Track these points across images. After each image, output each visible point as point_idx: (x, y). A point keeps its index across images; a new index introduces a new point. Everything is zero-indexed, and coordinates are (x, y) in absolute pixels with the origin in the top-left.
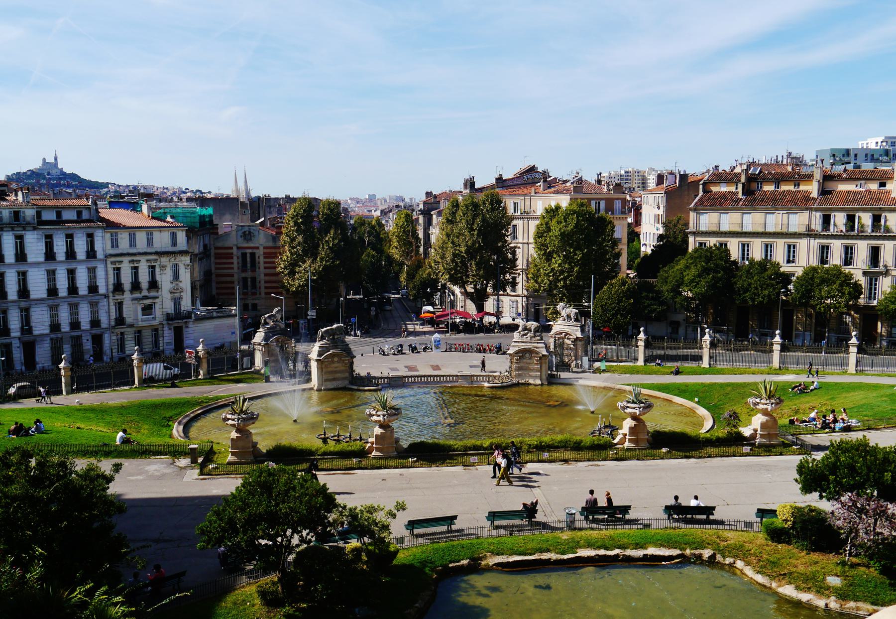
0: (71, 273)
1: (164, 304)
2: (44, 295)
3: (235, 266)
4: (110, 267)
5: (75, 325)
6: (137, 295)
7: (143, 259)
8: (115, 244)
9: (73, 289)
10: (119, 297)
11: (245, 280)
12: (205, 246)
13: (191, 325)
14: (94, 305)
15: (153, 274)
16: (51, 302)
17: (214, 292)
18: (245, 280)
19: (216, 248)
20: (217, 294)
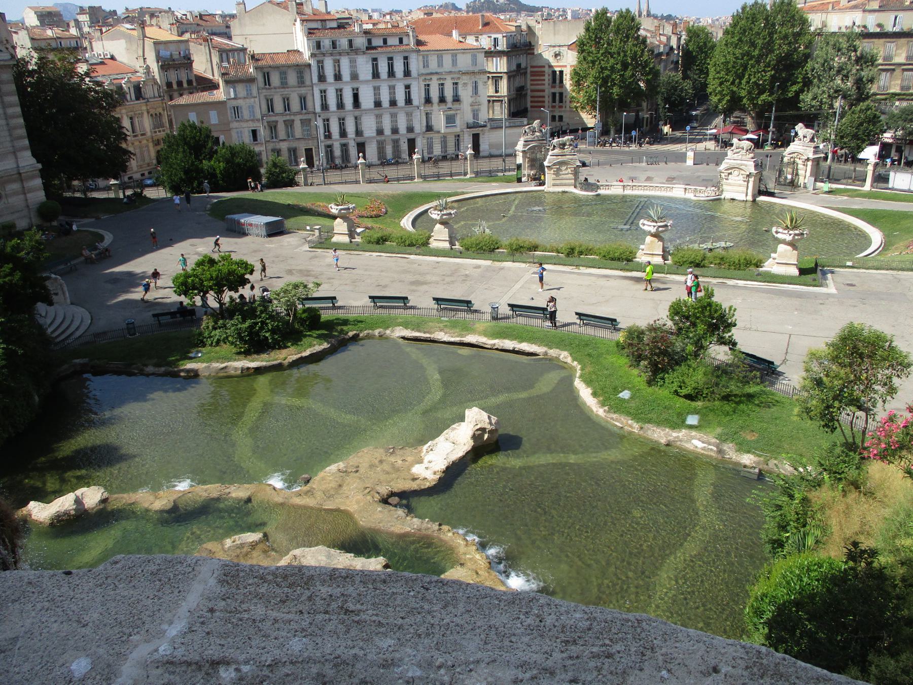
0: (392, 89)
1: (465, 115)
2: (372, 105)
3: (546, 82)
4: (422, 84)
5: (395, 131)
6: (443, 106)
7: (449, 78)
8: (426, 65)
9: (393, 103)
10: (428, 108)
11: (554, 94)
12: (519, 66)
13: (487, 134)
14: (409, 115)
15: (456, 90)
16: (377, 112)
17: (529, 105)
18: (554, 94)
19: (532, 67)
20: (532, 107)
